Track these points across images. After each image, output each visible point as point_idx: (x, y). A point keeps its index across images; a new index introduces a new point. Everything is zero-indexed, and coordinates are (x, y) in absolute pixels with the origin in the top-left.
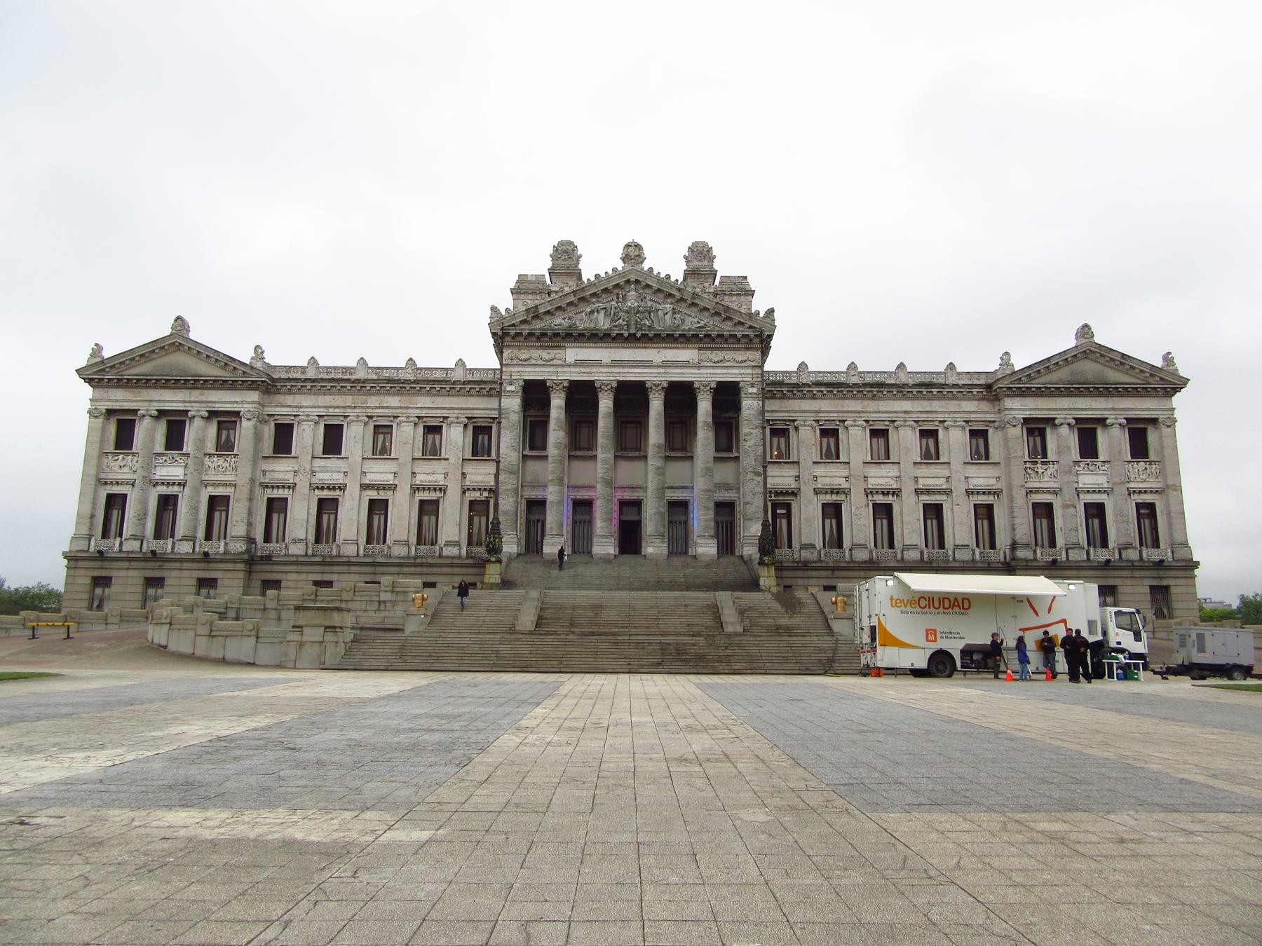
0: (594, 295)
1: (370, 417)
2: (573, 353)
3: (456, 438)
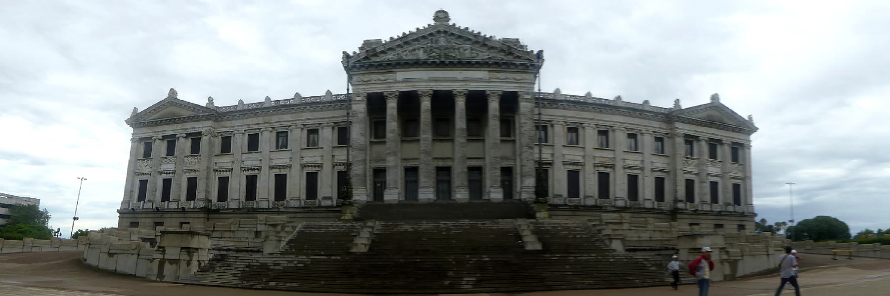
3: (328, 136)
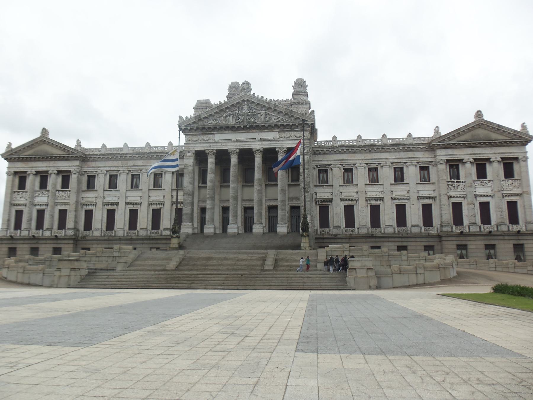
0: (227, 108)
1: (129, 171)
2: (218, 137)
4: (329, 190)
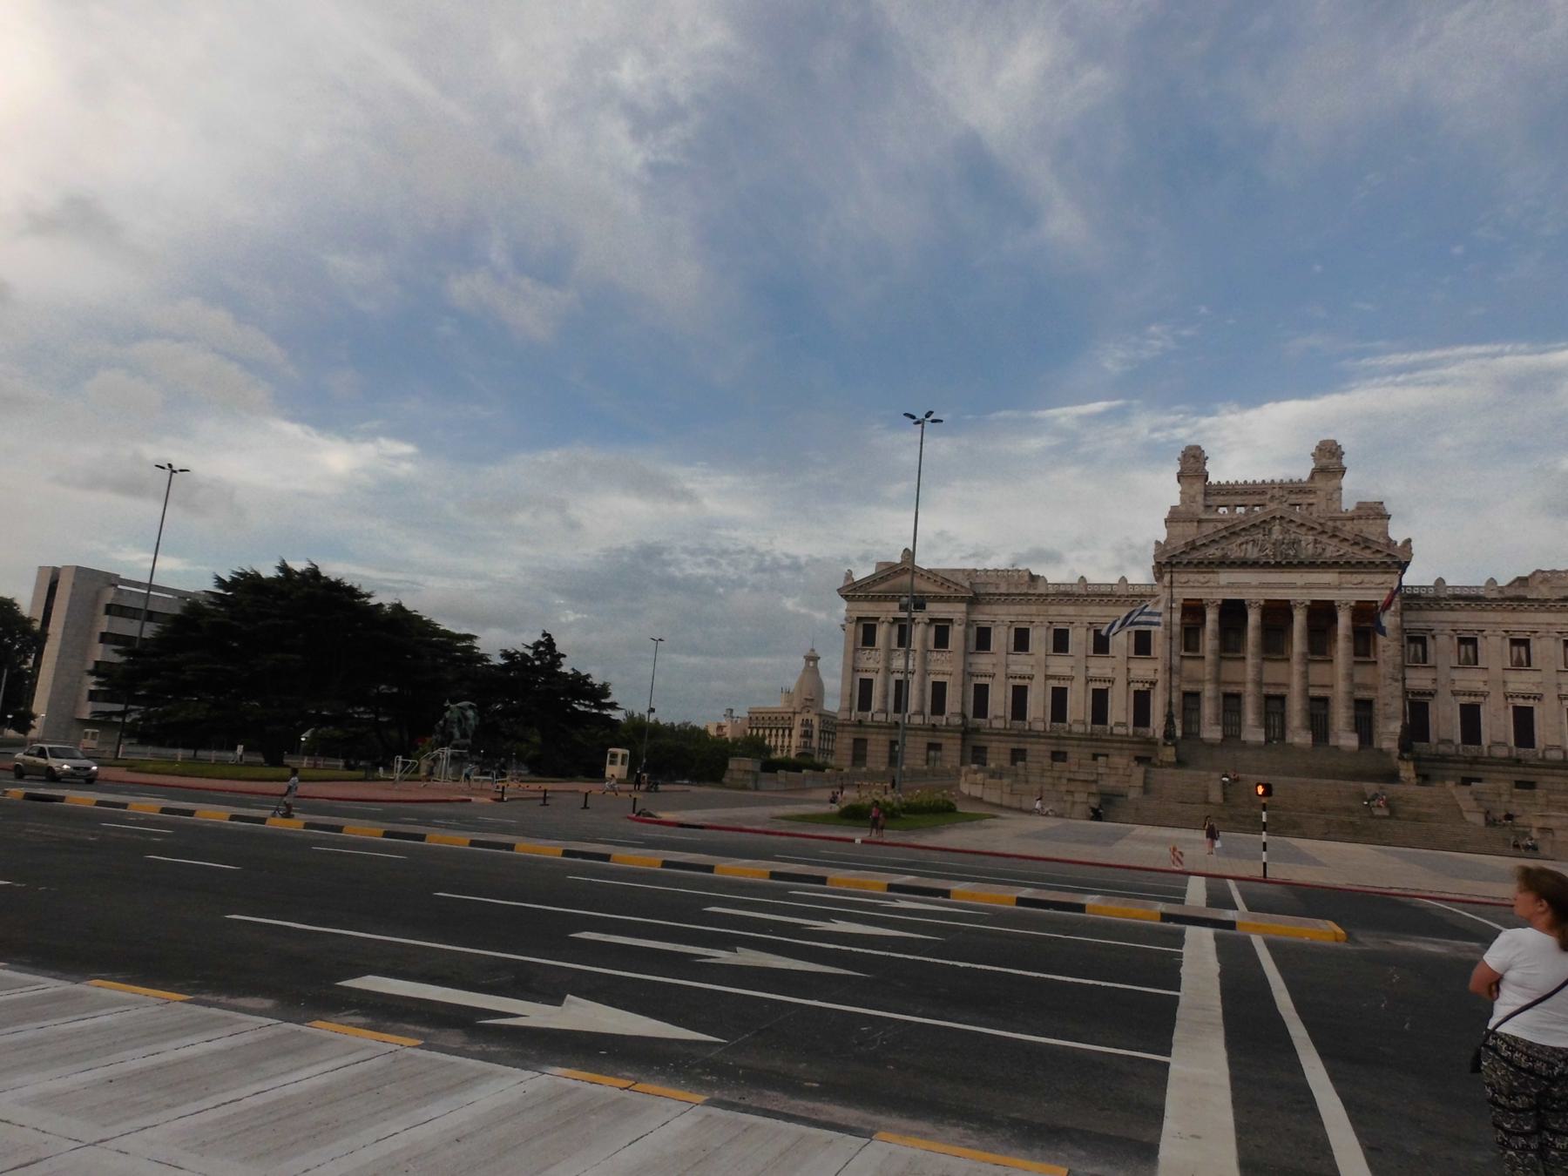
2: (1225, 577)
4: (1430, 675)
